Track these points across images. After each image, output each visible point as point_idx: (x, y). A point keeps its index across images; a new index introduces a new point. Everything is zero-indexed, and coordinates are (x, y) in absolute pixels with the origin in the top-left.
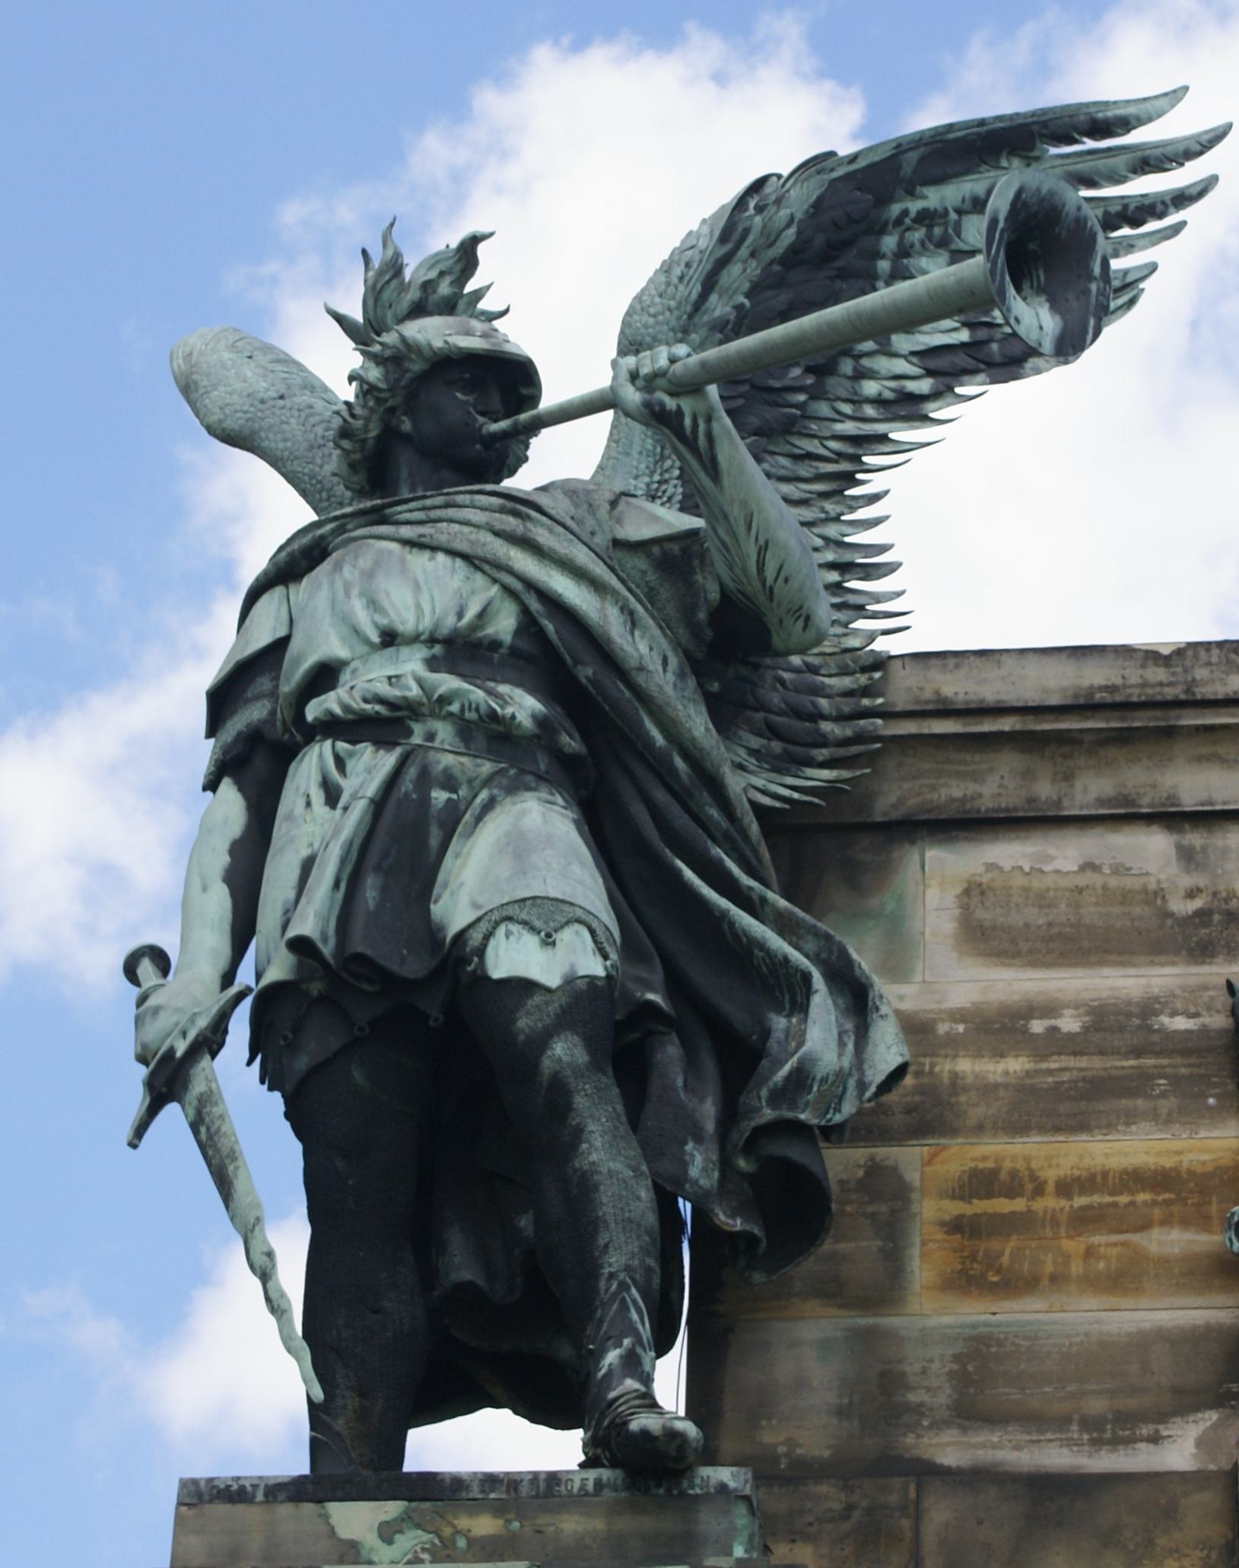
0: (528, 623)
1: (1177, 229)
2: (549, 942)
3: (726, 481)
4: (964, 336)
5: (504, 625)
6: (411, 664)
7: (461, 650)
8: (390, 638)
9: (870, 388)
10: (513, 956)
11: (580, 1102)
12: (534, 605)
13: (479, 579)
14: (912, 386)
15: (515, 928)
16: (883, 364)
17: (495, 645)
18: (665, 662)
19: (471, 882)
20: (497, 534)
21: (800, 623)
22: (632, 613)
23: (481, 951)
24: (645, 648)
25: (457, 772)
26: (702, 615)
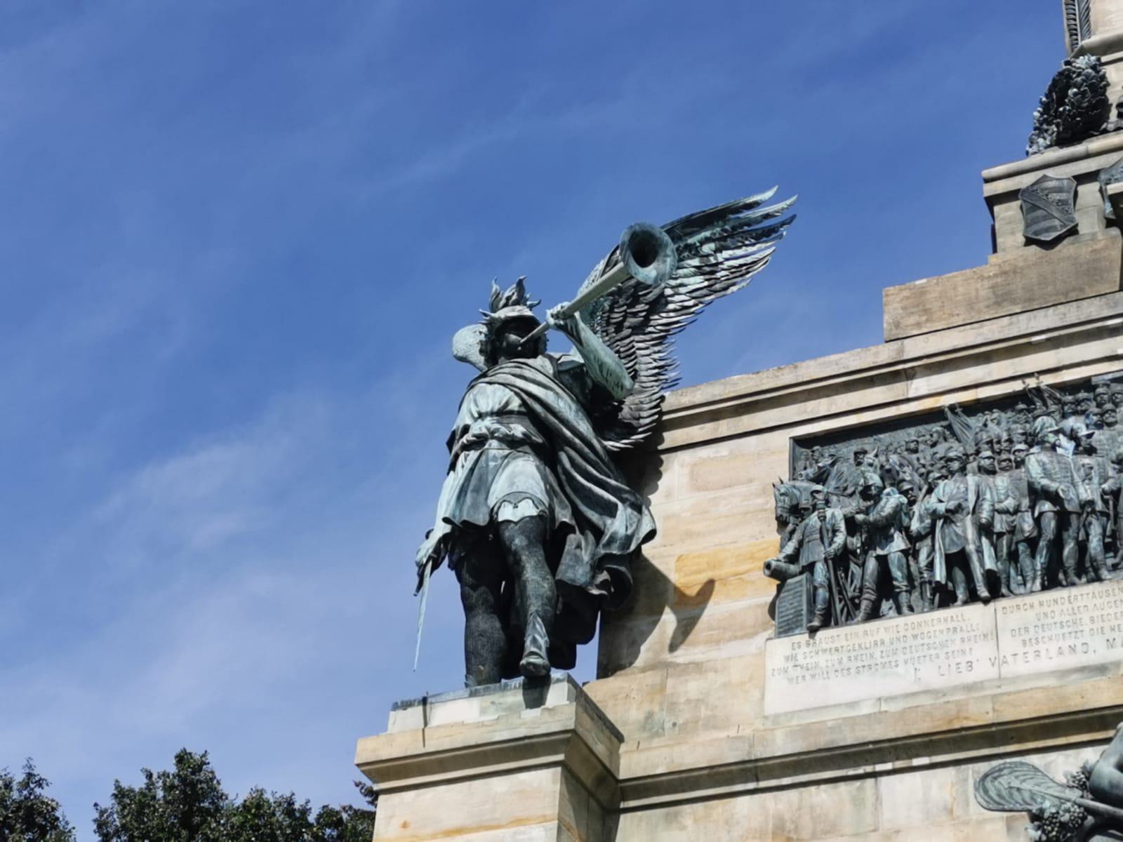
0: (524, 403)
2: (516, 507)
3: (585, 345)
4: (706, 283)
5: (515, 404)
6: (489, 423)
7: (502, 413)
8: (481, 416)
9: (671, 306)
10: (506, 513)
11: (524, 558)
12: (525, 397)
13: (507, 391)
14: (686, 304)
15: (506, 503)
16: (677, 298)
17: (511, 412)
18: (570, 408)
19: (498, 489)
20: (513, 375)
21: (620, 388)
22: (557, 394)
23: (497, 513)
24: (565, 405)
25: (497, 455)
26: (587, 391)
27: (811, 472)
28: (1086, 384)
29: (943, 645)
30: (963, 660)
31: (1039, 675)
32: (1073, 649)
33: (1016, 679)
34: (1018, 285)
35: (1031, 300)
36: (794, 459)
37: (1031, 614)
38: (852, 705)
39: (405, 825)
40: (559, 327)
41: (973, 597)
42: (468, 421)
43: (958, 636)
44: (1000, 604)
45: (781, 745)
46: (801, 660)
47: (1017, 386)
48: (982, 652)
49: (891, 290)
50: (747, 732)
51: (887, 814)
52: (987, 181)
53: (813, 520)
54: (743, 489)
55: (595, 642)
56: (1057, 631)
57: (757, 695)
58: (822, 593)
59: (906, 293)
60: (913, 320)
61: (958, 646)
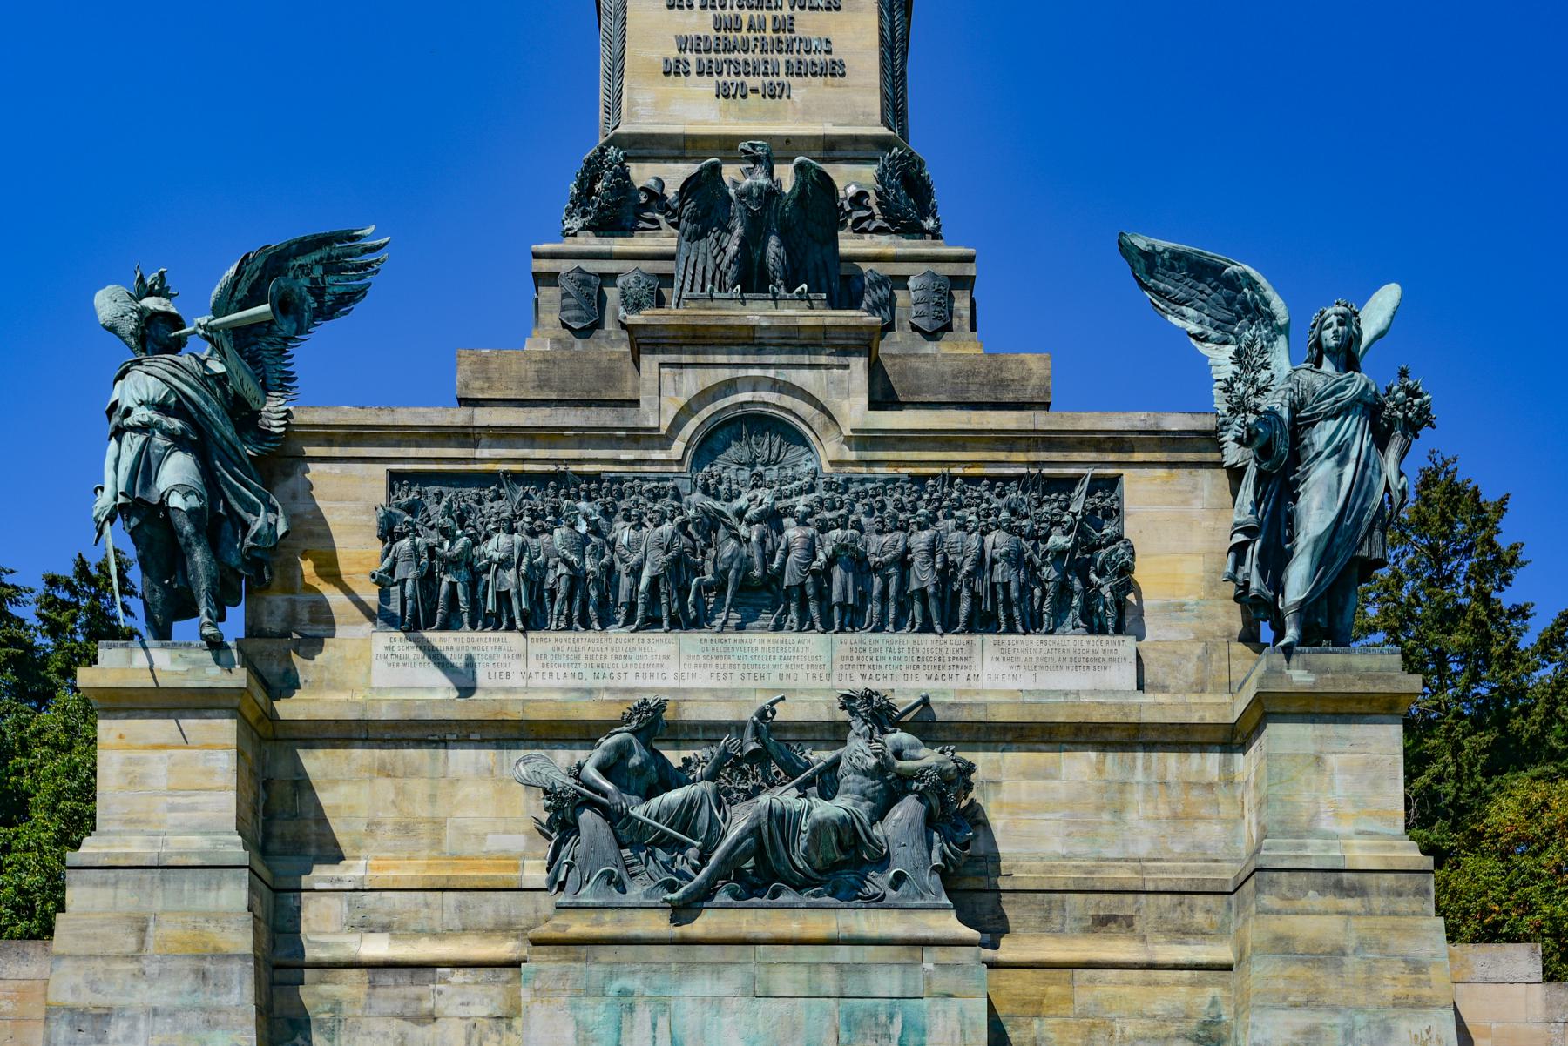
1: (377, 271)
27: (404, 501)
28: (596, 477)
29: (491, 657)
30: (504, 670)
31: (550, 689)
32: (573, 675)
33: (536, 690)
34: (556, 373)
35: (563, 390)
36: (391, 489)
37: (550, 646)
38: (431, 689)
39: (121, 736)
40: (206, 337)
41: (511, 627)
42: (131, 405)
43: (502, 653)
44: (531, 635)
45: (385, 713)
46: (396, 651)
47: (552, 468)
48: (516, 667)
49: (464, 353)
50: (359, 697)
51: (452, 767)
52: (537, 256)
53: (406, 542)
54: (352, 505)
55: (242, 605)
56: (565, 661)
57: (365, 669)
58: (409, 603)
59: (474, 358)
60: (478, 384)
61: (501, 660)
